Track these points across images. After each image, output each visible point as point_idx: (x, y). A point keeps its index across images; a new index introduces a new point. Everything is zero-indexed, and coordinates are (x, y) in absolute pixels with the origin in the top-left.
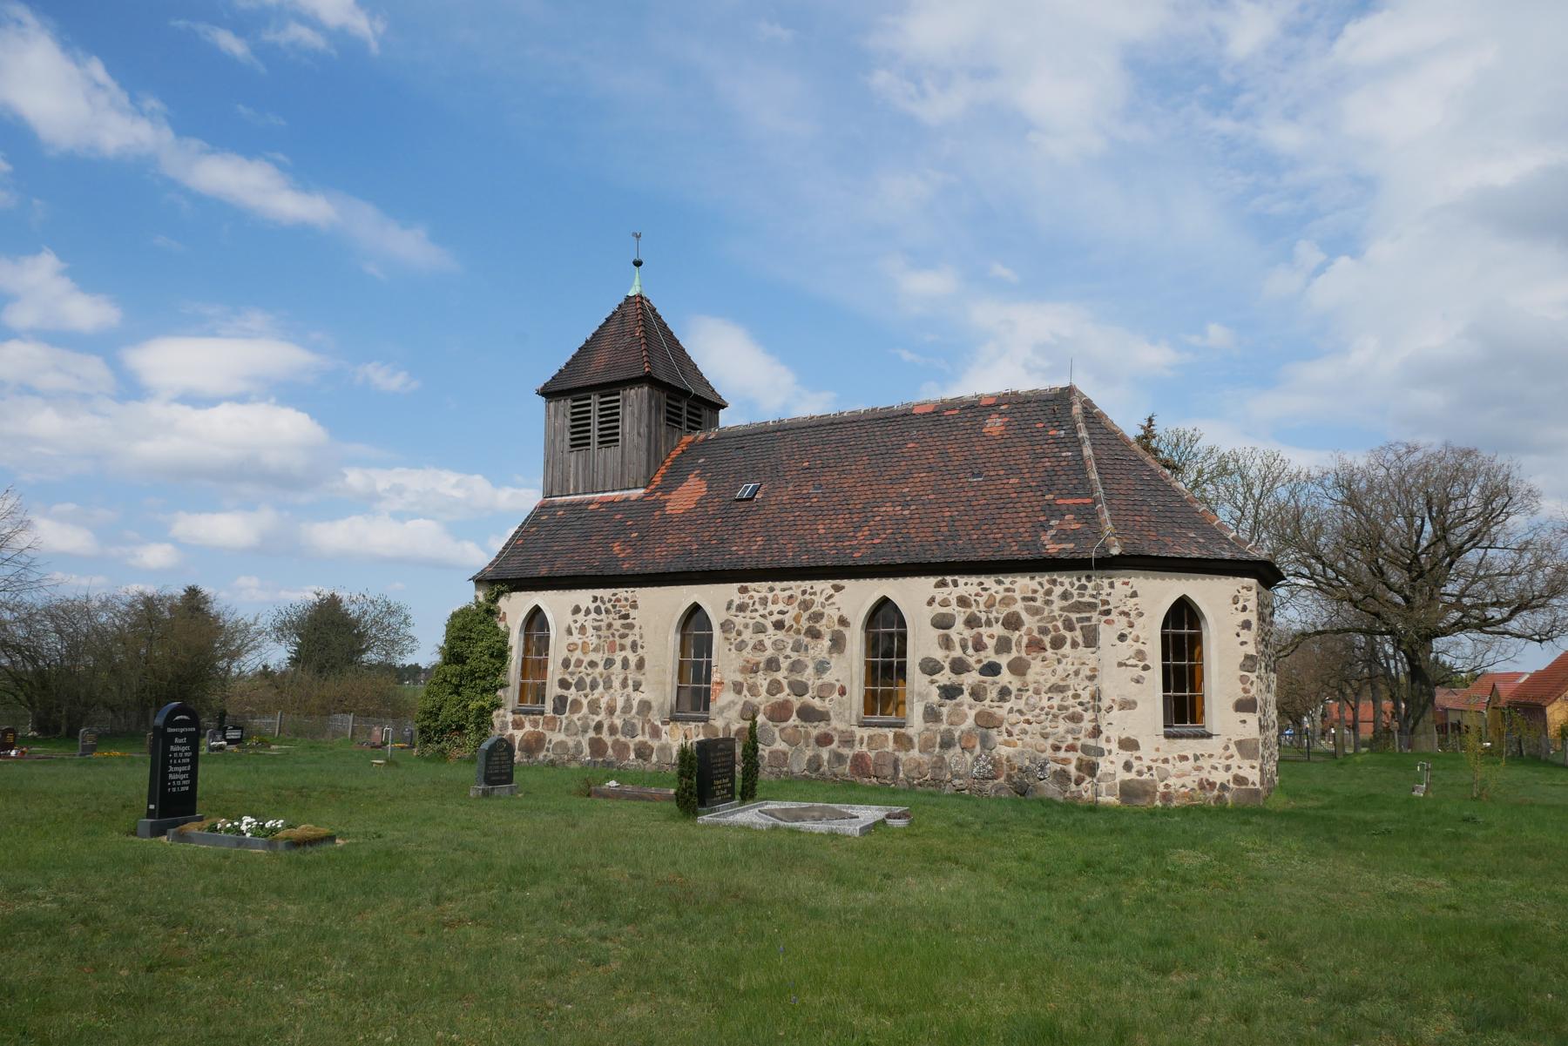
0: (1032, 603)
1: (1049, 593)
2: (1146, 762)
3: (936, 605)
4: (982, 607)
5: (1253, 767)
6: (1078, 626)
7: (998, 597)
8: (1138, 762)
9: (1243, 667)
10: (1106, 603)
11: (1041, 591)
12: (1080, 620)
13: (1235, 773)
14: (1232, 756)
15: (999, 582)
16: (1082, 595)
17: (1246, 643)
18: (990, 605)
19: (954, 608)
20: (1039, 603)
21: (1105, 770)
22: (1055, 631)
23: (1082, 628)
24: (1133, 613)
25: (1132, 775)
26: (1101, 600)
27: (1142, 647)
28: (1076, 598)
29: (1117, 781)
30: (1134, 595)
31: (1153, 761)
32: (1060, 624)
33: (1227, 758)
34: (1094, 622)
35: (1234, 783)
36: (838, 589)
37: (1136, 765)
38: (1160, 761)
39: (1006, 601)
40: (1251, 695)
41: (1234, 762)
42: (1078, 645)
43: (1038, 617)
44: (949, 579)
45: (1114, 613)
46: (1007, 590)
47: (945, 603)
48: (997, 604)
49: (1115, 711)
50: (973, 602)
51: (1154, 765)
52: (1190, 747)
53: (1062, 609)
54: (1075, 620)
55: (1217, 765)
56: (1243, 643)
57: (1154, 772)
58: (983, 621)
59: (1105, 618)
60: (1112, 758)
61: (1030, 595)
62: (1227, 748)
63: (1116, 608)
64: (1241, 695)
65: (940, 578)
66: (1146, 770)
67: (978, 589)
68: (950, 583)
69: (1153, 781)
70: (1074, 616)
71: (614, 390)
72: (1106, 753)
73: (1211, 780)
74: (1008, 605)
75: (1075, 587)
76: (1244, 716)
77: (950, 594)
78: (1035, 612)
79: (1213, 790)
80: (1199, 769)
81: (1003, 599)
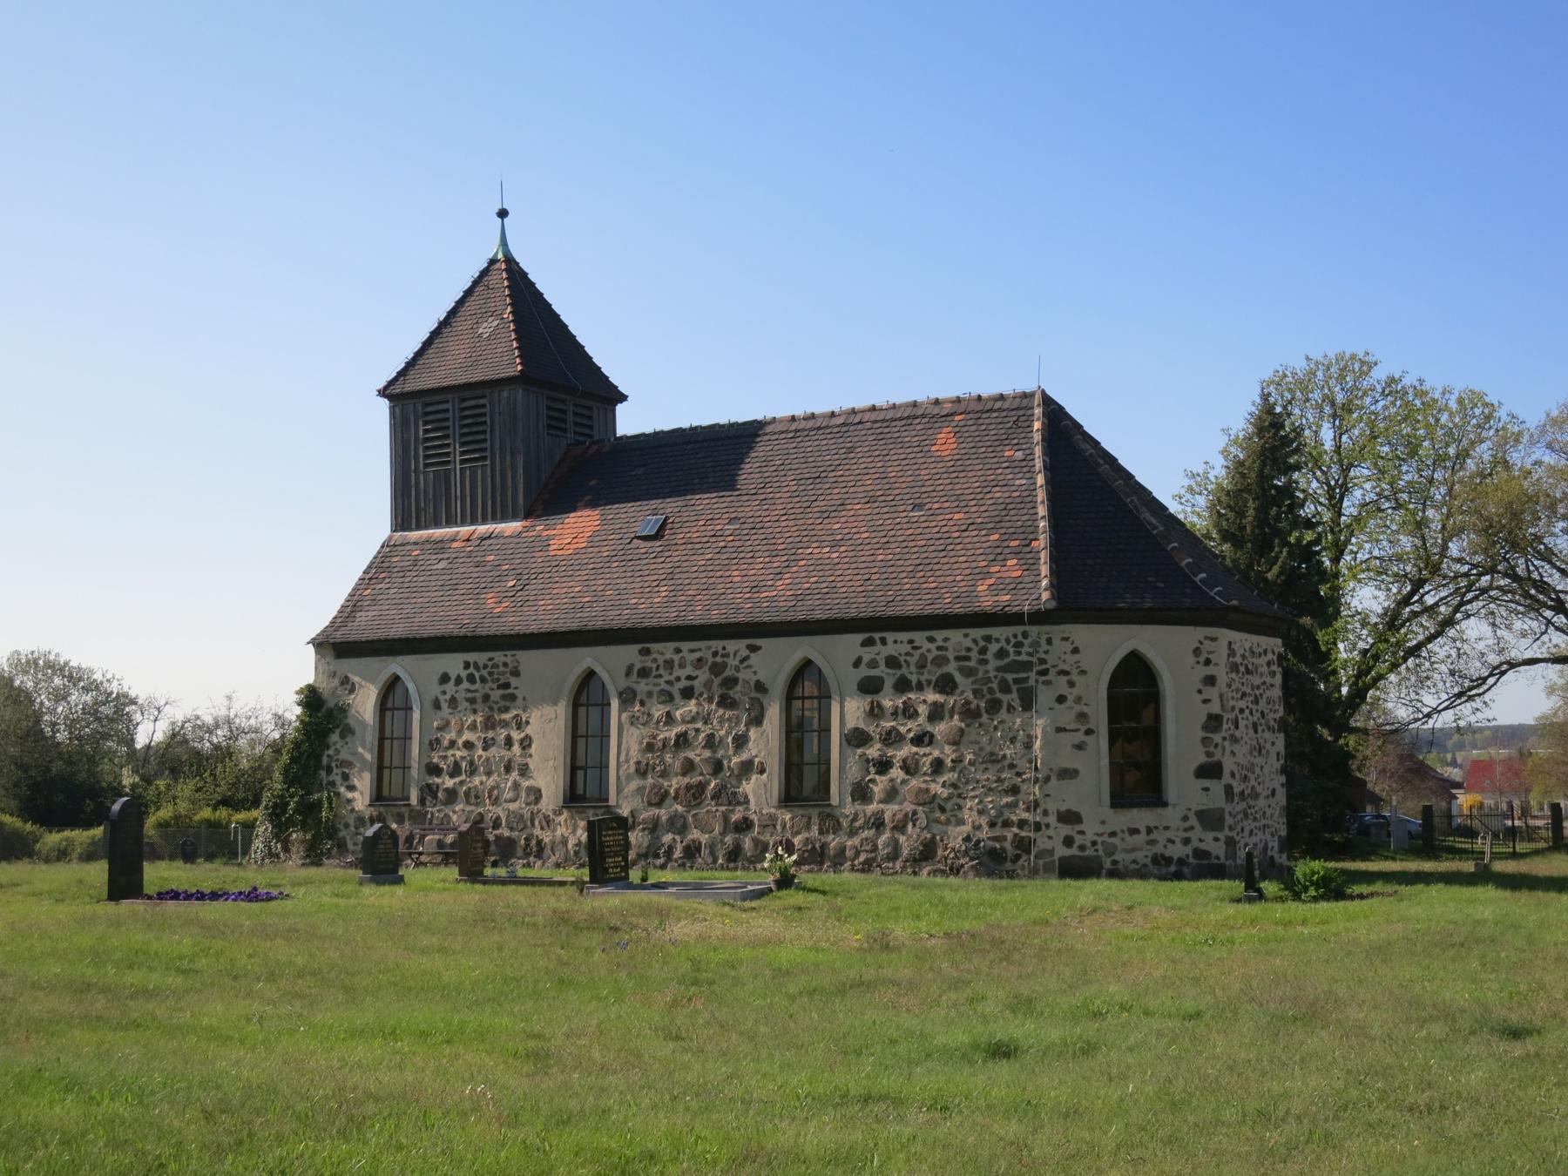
0: (967, 663)
1: (983, 651)
2: (1090, 837)
3: (863, 666)
4: (913, 668)
5: (1216, 839)
6: (1014, 688)
7: (930, 657)
8: (1080, 837)
9: (1205, 728)
10: (1043, 661)
11: (976, 649)
12: (1016, 681)
13: (1195, 846)
14: (1192, 828)
15: (931, 640)
16: (1019, 653)
17: (1209, 701)
18: (921, 666)
19: (881, 670)
20: (972, 664)
21: (1042, 846)
22: (989, 693)
23: (1018, 690)
24: (1075, 672)
25: (1074, 851)
26: (1039, 659)
27: (1085, 709)
28: (1012, 657)
29: (1056, 857)
30: (1076, 651)
31: (1097, 834)
32: (995, 686)
33: (1186, 830)
34: (1032, 682)
35: (1194, 857)
36: (754, 649)
37: (1079, 840)
38: (1106, 835)
39: (941, 661)
40: (1215, 759)
41: (1193, 835)
42: (1014, 708)
43: (972, 679)
44: (877, 636)
45: (1052, 672)
46: (939, 648)
47: (873, 664)
48: (929, 664)
49: (1053, 780)
50: (903, 663)
51: (1100, 840)
52: (1141, 817)
53: (998, 669)
54: (1011, 681)
55: (1174, 838)
56: (1206, 701)
57: (1099, 847)
58: (914, 684)
59: (1043, 678)
60: (1051, 832)
61: (963, 653)
62: (1185, 818)
63: (1054, 667)
64: (1203, 759)
65: (867, 635)
66: (1089, 845)
67: (908, 648)
68: (878, 641)
69: (1098, 857)
70: (1010, 677)
71: (479, 392)
72: (1043, 827)
73: (1167, 855)
74: (940, 666)
75: (1012, 644)
76: (1207, 783)
77: (878, 654)
78: (968, 672)
79: (1169, 866)
80: (1152, 842)
81: (936, 658)
